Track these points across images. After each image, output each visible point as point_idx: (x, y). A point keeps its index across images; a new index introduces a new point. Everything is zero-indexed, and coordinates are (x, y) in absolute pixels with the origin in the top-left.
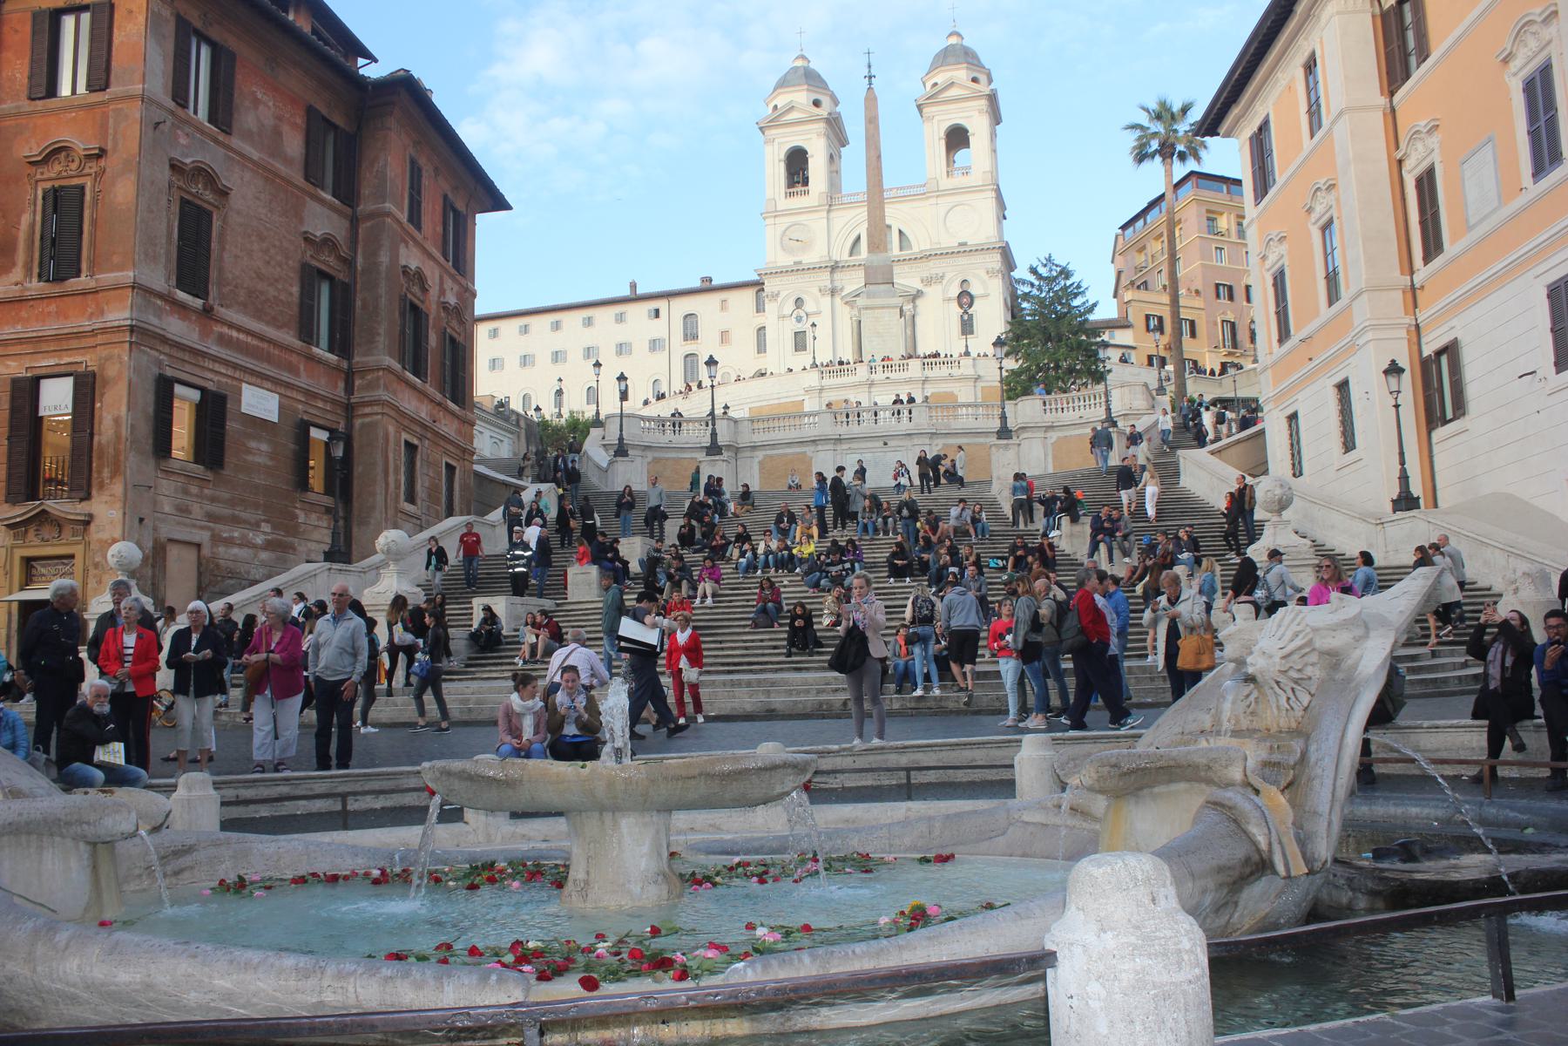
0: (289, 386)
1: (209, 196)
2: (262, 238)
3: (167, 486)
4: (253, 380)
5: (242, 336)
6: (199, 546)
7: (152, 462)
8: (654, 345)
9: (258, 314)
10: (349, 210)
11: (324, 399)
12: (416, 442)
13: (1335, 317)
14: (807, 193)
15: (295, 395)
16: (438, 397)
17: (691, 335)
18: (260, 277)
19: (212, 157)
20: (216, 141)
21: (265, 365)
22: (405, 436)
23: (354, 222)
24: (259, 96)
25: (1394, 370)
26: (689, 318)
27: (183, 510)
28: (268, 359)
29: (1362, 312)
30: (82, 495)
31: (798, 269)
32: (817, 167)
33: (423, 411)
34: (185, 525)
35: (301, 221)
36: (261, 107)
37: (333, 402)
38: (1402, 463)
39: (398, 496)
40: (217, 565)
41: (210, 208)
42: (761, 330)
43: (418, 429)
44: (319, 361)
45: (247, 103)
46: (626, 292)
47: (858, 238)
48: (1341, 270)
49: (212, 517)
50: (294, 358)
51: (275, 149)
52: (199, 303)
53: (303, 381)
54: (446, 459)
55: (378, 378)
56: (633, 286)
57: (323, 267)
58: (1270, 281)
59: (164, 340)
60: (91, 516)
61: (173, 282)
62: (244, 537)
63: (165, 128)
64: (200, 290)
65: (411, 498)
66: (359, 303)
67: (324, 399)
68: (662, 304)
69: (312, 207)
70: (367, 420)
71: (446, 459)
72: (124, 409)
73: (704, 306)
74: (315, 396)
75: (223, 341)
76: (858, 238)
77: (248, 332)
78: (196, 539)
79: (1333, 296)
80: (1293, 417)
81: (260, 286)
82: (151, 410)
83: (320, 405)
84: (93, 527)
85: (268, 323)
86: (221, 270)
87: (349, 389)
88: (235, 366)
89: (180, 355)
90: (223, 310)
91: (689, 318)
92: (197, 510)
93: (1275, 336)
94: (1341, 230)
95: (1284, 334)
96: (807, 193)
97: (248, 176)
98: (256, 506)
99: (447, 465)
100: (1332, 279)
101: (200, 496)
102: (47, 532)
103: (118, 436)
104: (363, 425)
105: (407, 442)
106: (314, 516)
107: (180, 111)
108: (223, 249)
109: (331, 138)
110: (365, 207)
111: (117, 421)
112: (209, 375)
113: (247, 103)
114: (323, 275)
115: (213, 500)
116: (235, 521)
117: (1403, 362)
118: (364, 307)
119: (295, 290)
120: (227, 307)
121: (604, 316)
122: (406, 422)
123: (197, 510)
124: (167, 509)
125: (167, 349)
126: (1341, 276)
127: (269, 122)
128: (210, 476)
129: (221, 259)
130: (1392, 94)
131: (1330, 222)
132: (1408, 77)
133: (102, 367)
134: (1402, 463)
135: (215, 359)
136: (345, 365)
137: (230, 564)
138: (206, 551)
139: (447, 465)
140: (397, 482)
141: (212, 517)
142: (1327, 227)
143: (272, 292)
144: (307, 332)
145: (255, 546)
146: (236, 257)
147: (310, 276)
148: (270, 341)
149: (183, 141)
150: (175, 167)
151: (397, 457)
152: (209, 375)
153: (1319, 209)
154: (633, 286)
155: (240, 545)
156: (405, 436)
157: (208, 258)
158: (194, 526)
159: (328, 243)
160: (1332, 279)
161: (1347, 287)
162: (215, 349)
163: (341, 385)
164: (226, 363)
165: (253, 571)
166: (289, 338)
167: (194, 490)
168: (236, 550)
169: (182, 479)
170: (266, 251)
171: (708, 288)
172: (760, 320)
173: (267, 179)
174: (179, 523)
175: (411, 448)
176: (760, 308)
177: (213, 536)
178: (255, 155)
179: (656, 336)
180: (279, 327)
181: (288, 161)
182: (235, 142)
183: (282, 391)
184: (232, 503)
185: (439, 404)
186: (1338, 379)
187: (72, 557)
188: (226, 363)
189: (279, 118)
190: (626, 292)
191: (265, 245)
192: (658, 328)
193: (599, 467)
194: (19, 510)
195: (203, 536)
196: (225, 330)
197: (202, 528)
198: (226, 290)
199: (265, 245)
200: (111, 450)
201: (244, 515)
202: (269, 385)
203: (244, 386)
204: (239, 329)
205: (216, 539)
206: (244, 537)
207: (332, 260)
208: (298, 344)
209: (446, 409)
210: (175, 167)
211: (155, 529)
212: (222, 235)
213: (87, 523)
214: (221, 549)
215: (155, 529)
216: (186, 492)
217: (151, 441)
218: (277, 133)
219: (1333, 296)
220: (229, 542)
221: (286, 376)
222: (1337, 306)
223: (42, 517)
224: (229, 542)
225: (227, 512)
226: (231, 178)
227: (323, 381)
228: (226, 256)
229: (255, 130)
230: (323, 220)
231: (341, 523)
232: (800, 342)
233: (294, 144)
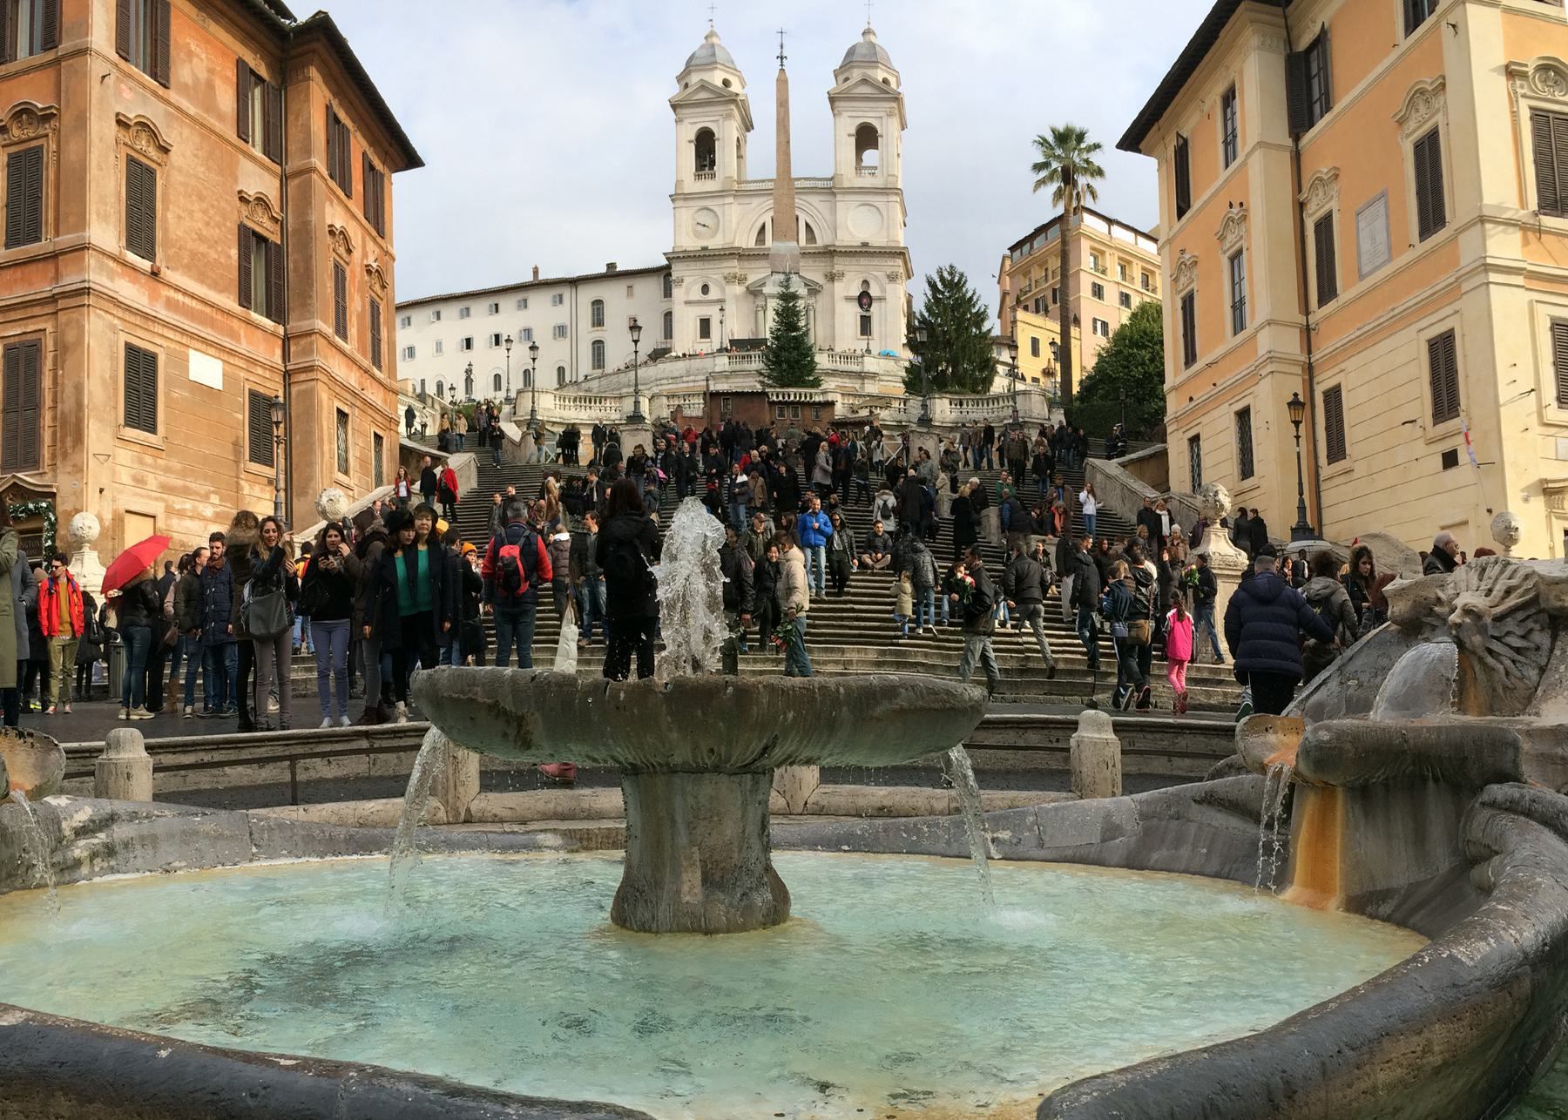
0: (232, 352)
1: (153, 152)
2: (201, 198)
3: (124, 455)
4: (199, 345)
5: (187, 300)
8: (561, 331)
9: (202, 278)
10: (277, 168)
11: (263, 366)
12: (346, 410)
13: (1242, 344)
14: (713, 176)
15: (236, 361)
16: (367, 363)
17: (598, 321)
18: (201, 238)
19: (154, 112)
20: (155, 94)
21: (209, 330)
22: (337, 404)
23: (284, 179)
24: (193, 47)
25: (1295, 404)
26: (598, 304)
27: (139, 481)
28: (212, 323)
29: (1265, 342)
31: (704, 256)
32: (725, 154)
33: (352, 378)
35: (236, 180)
36: (195, 60)
37: (272, 369)
38: (1301, 494)
39: (332, 465)
41: (153, 166)
42: (668, 316)
43: (349, 397)
44: (257, 327)
45: (182, 55)
46: (528, 278)
47: (763, 227)
48: (1247, 300)
49: (166, 489)
50: (235, 324)
51: (210, 105)
52: (146, 265)
53: (243, 347)
54: (375, 429)
55: (312, 343)
56: (536, 271)
57: (258, 229)
58: (1179, 304)
59: (118, 303)
61: (123, 243)
62: (195, 509)
63: (109, 81)
64: (149, 254)
65: (346, 473)
66: (291, 266)
67: (263, 366)
68: (566, 292)
69: (246, 166)
70: (303, 387)
71: (375, 429)
73: (613, 295)
74: (254, 362)
75: (171, 305)
76: (763, 227)
77: (193, 296)
79: (1239, 325)
80: (1195, 440)
81: (203, 248)
83: (260, 371)
85: (210, 287)
86: (166, 230)
87: (286, 356)
88: (183, 332)
89: (132, 318)
90: (169, 272)
91: (598, 304)
92: (152, 481)
93: (1183, 360)
94: (1250, 261)
95: (1190, 358)
96: (713, 176)
97: (186, 132)
98: (206, 477)
99: (376, 435)
100: (1238, 306)
104: (299, 393)
105: (339, 411)
106: (257, 488)
107: (122, 64)
108: (166, 209)
109: (257, 92)
110: (294, 164)
112: (158, 341)
113: (182, 55)
114: (261, 239)
115: (167, 470)
116: (185, 492)
117: (1301, 398)
118: (295, 270)
119: (234, 252)
120: (174, 269)
121: (508, 303)
122: (338, 390)
123: (152, 481)
125: (120, 313)
126: (1247, 307)
127: (203, 75)
129: (165, 219)
130: (1296, 138)
131: (1239, 252)
132: (1312, 125)
134: (1301, 494)
135: (166, 324)
136: (281, 330)
138: (161, 524)
139: (376, 435)
140: (331, 450)
141: (166, 489)
142: (1236, 257)
143: (213, 255)
144: (245, 299)
145: (205, 519)
146: (179, 217)
147: (250, 240)
148: (212, 306)
149: (127, 95)
150: (121, 123)
151: (328, 421)
152: (158, 341)
153: (1230, 238)
154: (536, 271)
155: (191, 518)
156: (337, 404)
157: (154, 218)
158: (149, 497)
159: (261, 201)
160: (1238, 306)
161: (1253, 319)
162: (163, 314)
163: (279, 352)
164: (174, 328)
166: (230, 302)
167: (149, 460)
168: (188, 523)
170: (205, 212)
171: (613, 274)
172: (664, 307)
173: (202, 135)
174: (136, 494)
175: (342, 416)
176: (668, 293)
178: (192, 110)
179: (560, 322)
180: (221, 291)
181: (221, 117)
182: (172, 95)
183: (226, 357)
184: (183, 474)
185: (366, 372)
186: (1239, 406)
188: (174, 328)
189: (211, 71)
190: (529, 278)
191: (204, 205)
192: (561, 315)
193: (512, 442)
196: (172, 293)
197: (157, 499)
198: (171, 252)
199: (204, 205)
201: (193, 486)
202: (212, 351)
203: (191, 352)
204: (185, 293)
205: (170, 511)
206: (195, 509)
207: (268, 224)
208: (238, 309)
209: (373, 377)
210: (121, 123)
212: (165, 194)
214: (175, 522)
218: (210, 86)
219: (1239, 325)
220: (181, 514)
221: (228, 343)
222: (1241, 336)
224: (181, 514)
225: (180, 483)
226: (171, 134)
227: (262, 348)
228: (170, 215)
229: (190, 82)
230: (259, 180)
231: (282, 494)
232: (705, 327)
233: (226, 99)
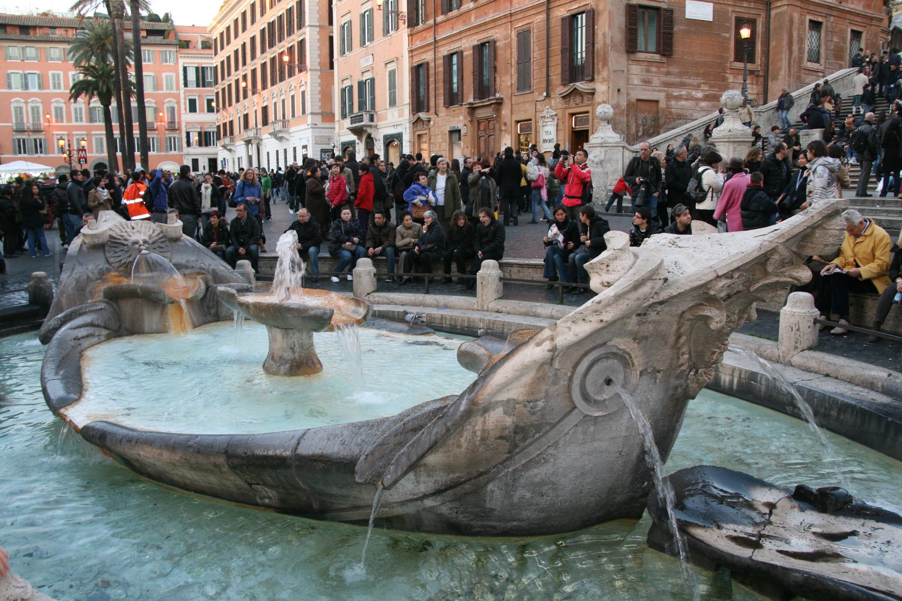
6: (657, 102)
7: (625, 56)
30: (590, 78)
34: (649, 90)
40: (670, 113)
60: (594, 89)
72: (607, 28)
78: (655, 98)
82: (623, 26)
84: (596, 96)
92: (656, 81)
101: (658, 73)
102: (578, 99)
103: (605, 44)
111: (604, 35)
115: (668, 74)
124: (636, 82)
128: (664, 59)
133: (597, 5)
137: (680, 111)
138: (662, 105)
158: (654, 90)
165: (695, 115)
169: (646, 63)
177: (667, 95)
187: (588, 112)
194: (566, 89)
195: (660, 96)
197: (659, 91)
200: (602, 53)
211: (628, 94)
213: (593, 94)
215: (628, 94)
216: (648, 71)
217: (624, 44)
223: (575, 91)
